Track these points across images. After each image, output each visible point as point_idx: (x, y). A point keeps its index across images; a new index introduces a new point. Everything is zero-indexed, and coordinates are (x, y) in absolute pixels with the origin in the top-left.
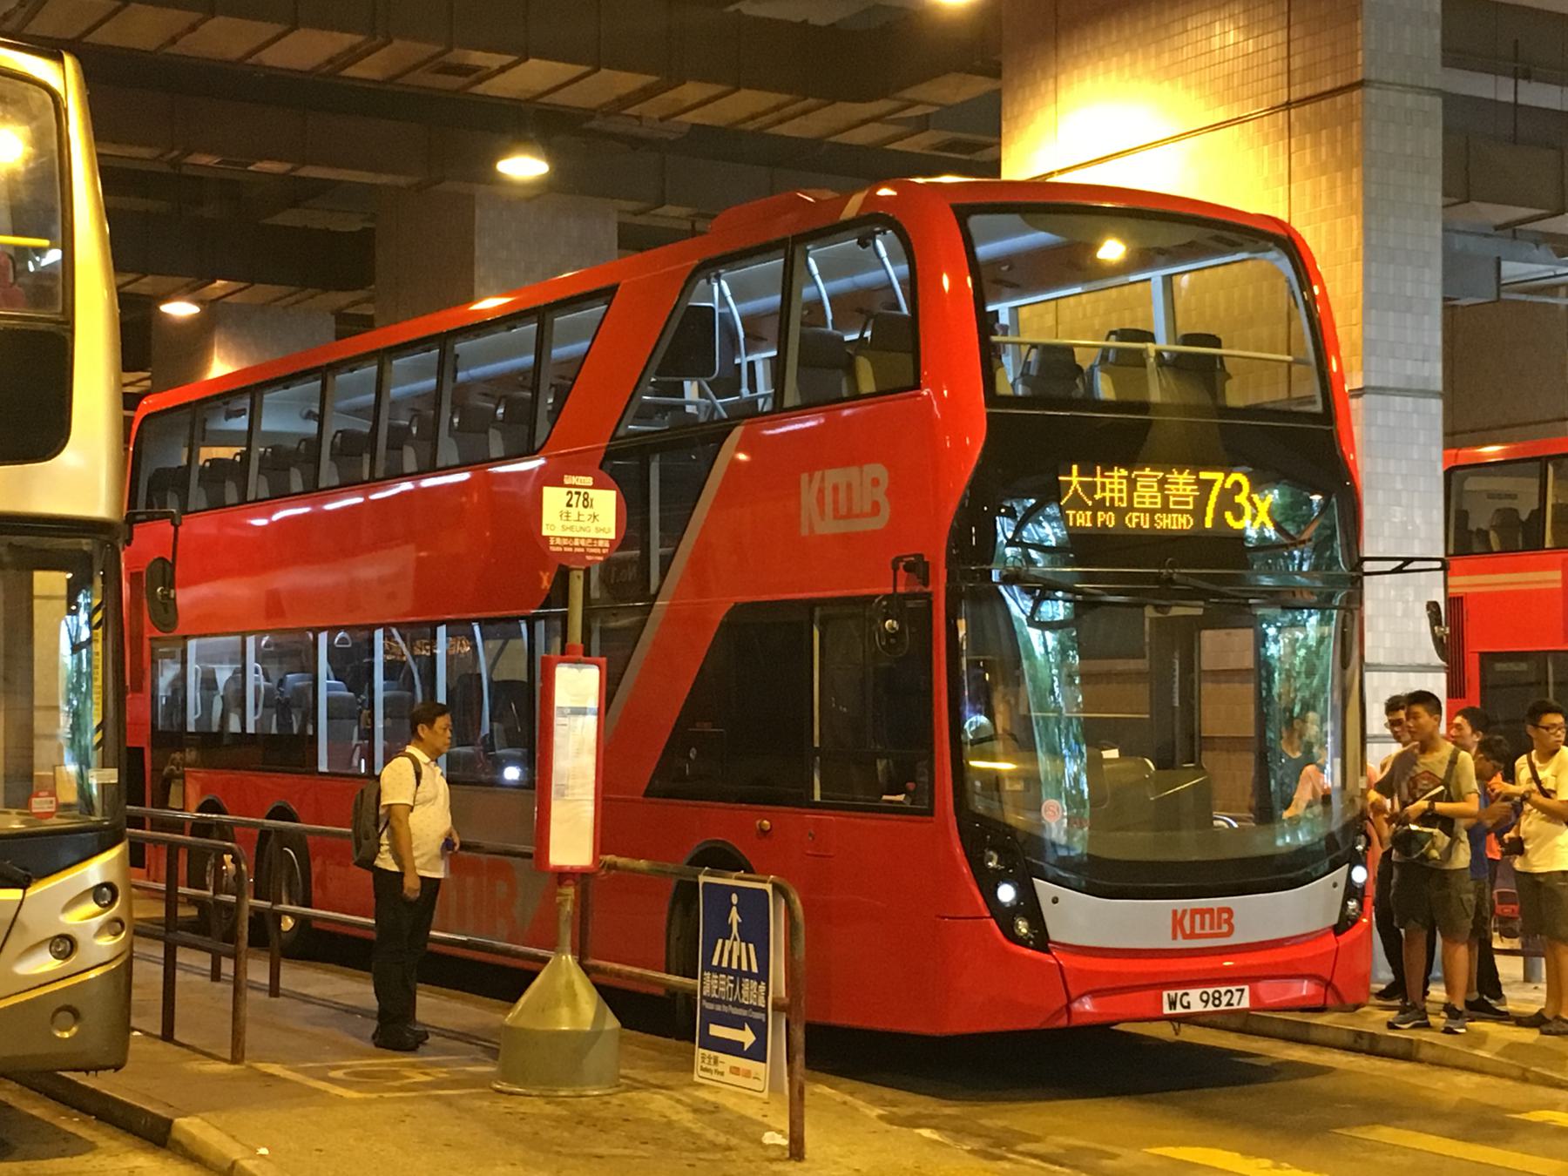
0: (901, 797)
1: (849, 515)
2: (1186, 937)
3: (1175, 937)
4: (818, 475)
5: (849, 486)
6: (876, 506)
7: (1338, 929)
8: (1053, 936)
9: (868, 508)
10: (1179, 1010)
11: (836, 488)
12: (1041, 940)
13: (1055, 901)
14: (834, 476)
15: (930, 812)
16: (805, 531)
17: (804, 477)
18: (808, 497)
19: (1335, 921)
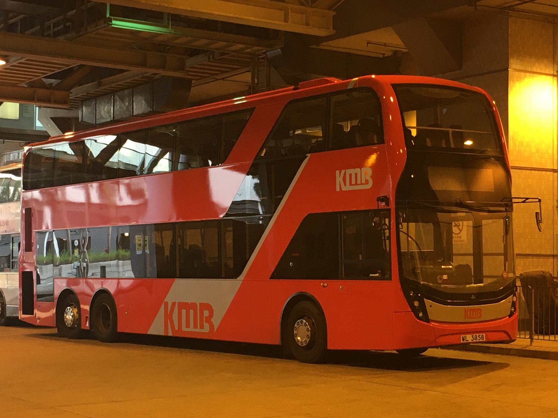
0: (377, 275)
1: (356, 184)
2: (468, 318)
3: (465, 318)
4: (343, 171)
5: (356, 174)
6: (367, 182)
7: (510, 316)
8: (430, 317)
9: (363, 182)
10: (465, 341)
11: (350, 175)
12: (426, 319)
13: (431, 306)
14: (349, 171)
15: (390, 279)
16: (338, 189)
17: (337, 172)
18: (339, 180)
19: (509, 313)
